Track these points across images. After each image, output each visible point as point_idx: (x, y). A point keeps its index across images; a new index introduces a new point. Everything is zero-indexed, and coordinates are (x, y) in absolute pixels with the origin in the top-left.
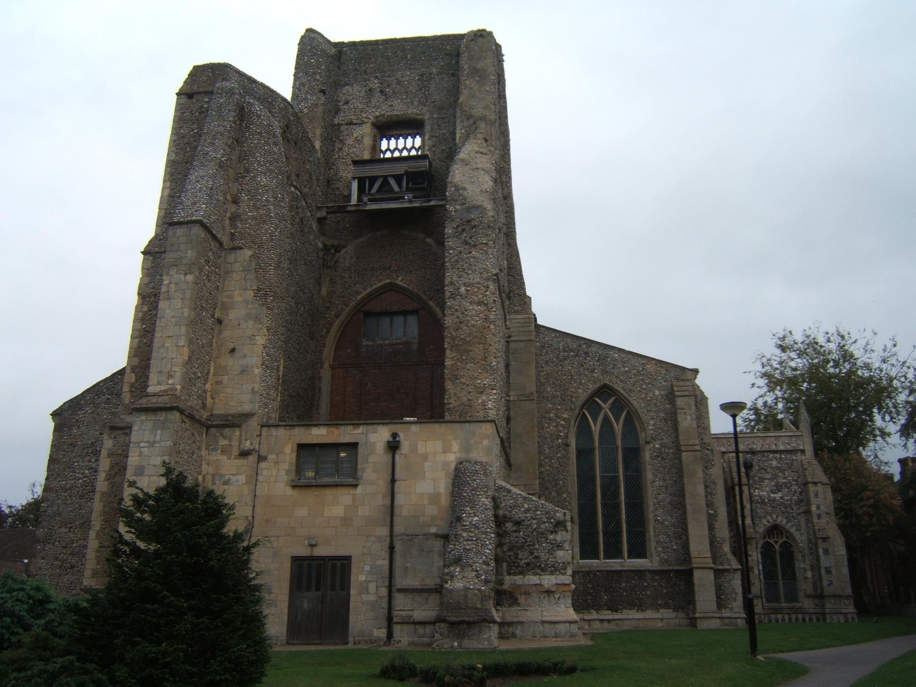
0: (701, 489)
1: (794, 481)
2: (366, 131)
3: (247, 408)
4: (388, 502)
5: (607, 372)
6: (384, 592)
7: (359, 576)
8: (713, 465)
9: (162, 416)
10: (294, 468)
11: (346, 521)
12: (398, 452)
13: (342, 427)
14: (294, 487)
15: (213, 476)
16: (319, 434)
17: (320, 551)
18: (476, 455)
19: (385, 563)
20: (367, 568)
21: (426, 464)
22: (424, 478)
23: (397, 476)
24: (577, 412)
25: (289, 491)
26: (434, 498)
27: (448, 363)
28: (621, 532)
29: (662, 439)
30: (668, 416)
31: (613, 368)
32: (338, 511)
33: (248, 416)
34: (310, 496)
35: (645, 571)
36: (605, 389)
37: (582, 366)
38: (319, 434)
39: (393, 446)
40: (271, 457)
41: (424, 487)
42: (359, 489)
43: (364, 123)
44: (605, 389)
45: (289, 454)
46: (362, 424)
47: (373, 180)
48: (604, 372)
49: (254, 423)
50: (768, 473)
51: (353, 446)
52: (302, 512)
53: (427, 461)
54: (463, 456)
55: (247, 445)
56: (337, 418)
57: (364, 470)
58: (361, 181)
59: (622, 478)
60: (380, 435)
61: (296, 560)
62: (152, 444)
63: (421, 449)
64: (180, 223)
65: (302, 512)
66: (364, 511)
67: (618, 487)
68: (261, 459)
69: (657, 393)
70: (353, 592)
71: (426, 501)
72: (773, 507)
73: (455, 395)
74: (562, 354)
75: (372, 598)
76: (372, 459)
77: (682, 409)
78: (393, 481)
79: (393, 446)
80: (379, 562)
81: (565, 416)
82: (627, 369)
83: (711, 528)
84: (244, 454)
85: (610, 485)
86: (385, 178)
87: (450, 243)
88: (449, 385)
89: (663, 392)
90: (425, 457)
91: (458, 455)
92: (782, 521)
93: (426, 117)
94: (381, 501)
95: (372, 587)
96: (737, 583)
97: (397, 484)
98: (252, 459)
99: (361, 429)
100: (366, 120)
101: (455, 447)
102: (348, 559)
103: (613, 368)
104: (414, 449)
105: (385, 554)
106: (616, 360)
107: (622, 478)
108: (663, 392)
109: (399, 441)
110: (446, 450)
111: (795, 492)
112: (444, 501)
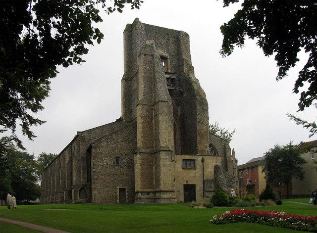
7: (197, 188)
9: (168, 153)
11: (194, 177)
14: (183, 169)
16: (187, 157)
18: (218, 164)
26: (211, 172)
27: (198, 139)
32: (192, 175)
34: (186, 171)
39: (203, 161)
41: (209, 170)
45: (181, 160)
51: (194, 160)
54: (216, 164)
60: (200, 158)
61: (184, 185)
62: (166, 159)
64: (163, 101)
66: (197, 175)
68: (176, 162)
73: (200, 147)
76: (198, 163)
79: (203, 161)
87: (198, 108)
88: (198, 145)
90: (209, 163)
93: (169, 57)
98: (174, 162)
102: (195, 185)
110: (213, 162)
112: (213, 173)
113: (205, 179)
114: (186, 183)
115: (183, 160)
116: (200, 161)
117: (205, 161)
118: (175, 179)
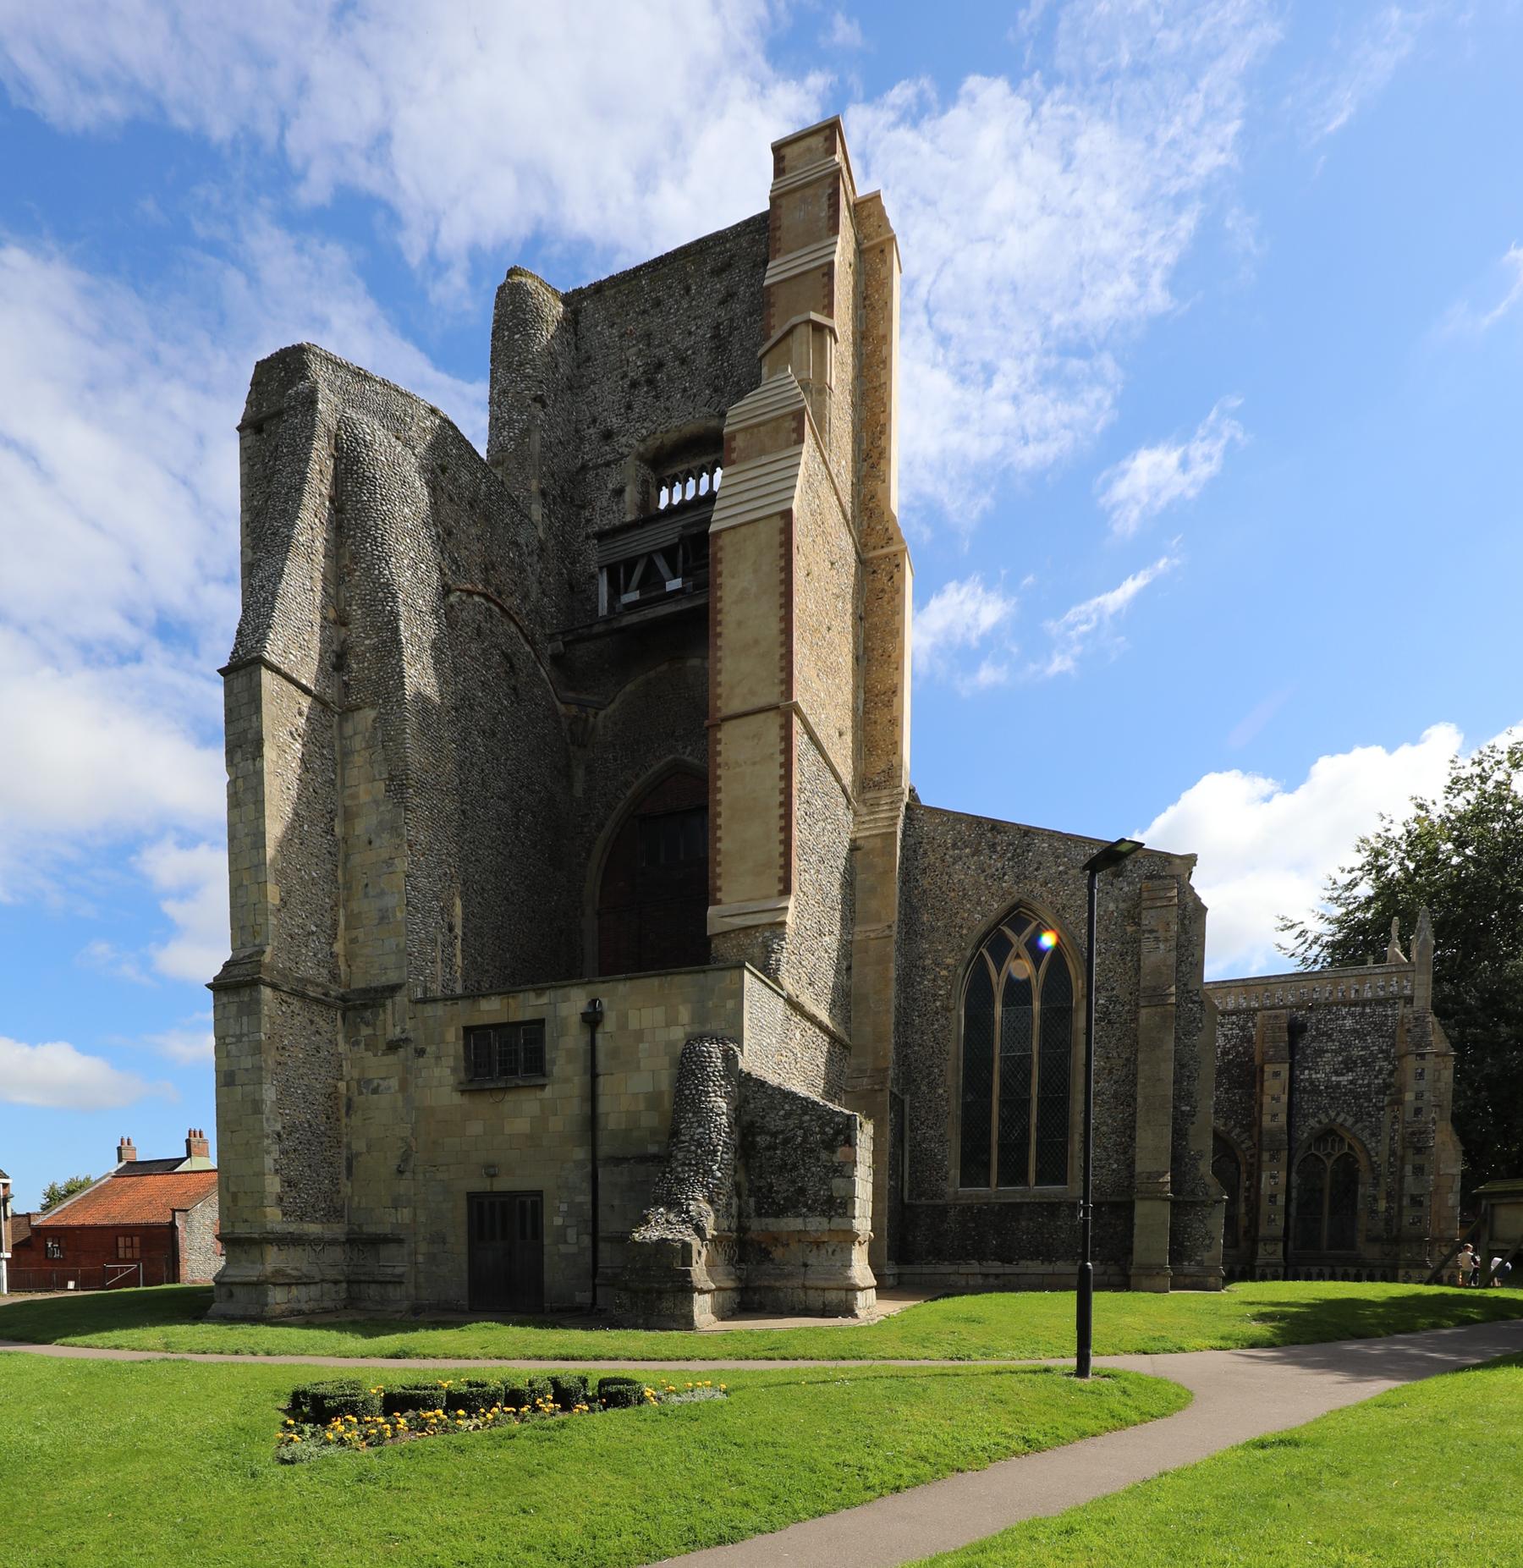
0: (1168, 1070)
1: (1382, 1051)
2: (629, 475)
3: (393, 977)
4: (587, 1108)
5: (1026, 878)
6: (586, 1240)
7: (554, 1220)
8: (1200, 1030)
10: (462, 1064)
12: (600, 1029)
13: (521, 995)
14: (463, 1092)
15: (359, 1081)
17: (503, 1184)
19: (585, 1199)
20: (564, 1207)
21: (641, 1046)
22: (638, 1068)
23: (601, 1068)
24: (968, 953)
25: (457, 1099)
28: (1028, 1144)
29: (1113, 989)
30: (1127, 946)
31: (1037, 870)
32: (521, 1125)
33: (393, 989)
35: (1060, 1204)
36: (1021, 909)
37: (984, 871)
38: (492, 1010)
39: (592, 1019)
40: (430, 1049)
42: (548, 1089)
43: (623, 456)
44: (1021, 909)
46: (548, 988)
47: (630, 564)
48: (1019, 878)
49: (401, 998)
50: (1333, 1041)
52: (475, 1128)
53: (642, 1042)
55: (394, 1033)
56: (513, 980)
57: (554, 1062)
58: (612, 570)
59: (1035, 1059)
60: (574, 1002)
63: (633, 1024)
65: (475, 1128)
66: (556, 1124)
67: (1029, 1074)
69: (1112, 906)
70: (547, 1241)
71: (642, 1106)
72: (1332, 1098)
74: (951, 853)
75: (573, 1249)
77: (1151, 931)
78: (594, 1076)
79: (592, 1019)
80: (579, 1199)
81: (949, 961)
82: (1061, 868)
83: (1179, 1134)
84: (393, 1046)
85: (1017, 1069)
86: (649, 556)
89: (1122, 905)
90: (639, 1036)
91: (688, 1029)
92: (1345, 1120)
94: (575, 1108)
95: (571, 1234)
96: (1217, 1223)
97: (601, 1080)
99: (544, 1000)
100: (626, 450)
101: (684, 1014)
102: (539, 1193)
103: (1037, 870)
104: (623, 1025)
105: (586, 1186)
106: (1043, 853)
107: (1035, 1059)
108: (1122, 905)
109: (601, 1013)
110: (671, 1022)
111: (1381, 1071)
113: (604, 1150)
114: (480, 1185)
115: (468, 1030)
116: (575, 1019)
117: (609, 1024)
118: (406, 1158)
